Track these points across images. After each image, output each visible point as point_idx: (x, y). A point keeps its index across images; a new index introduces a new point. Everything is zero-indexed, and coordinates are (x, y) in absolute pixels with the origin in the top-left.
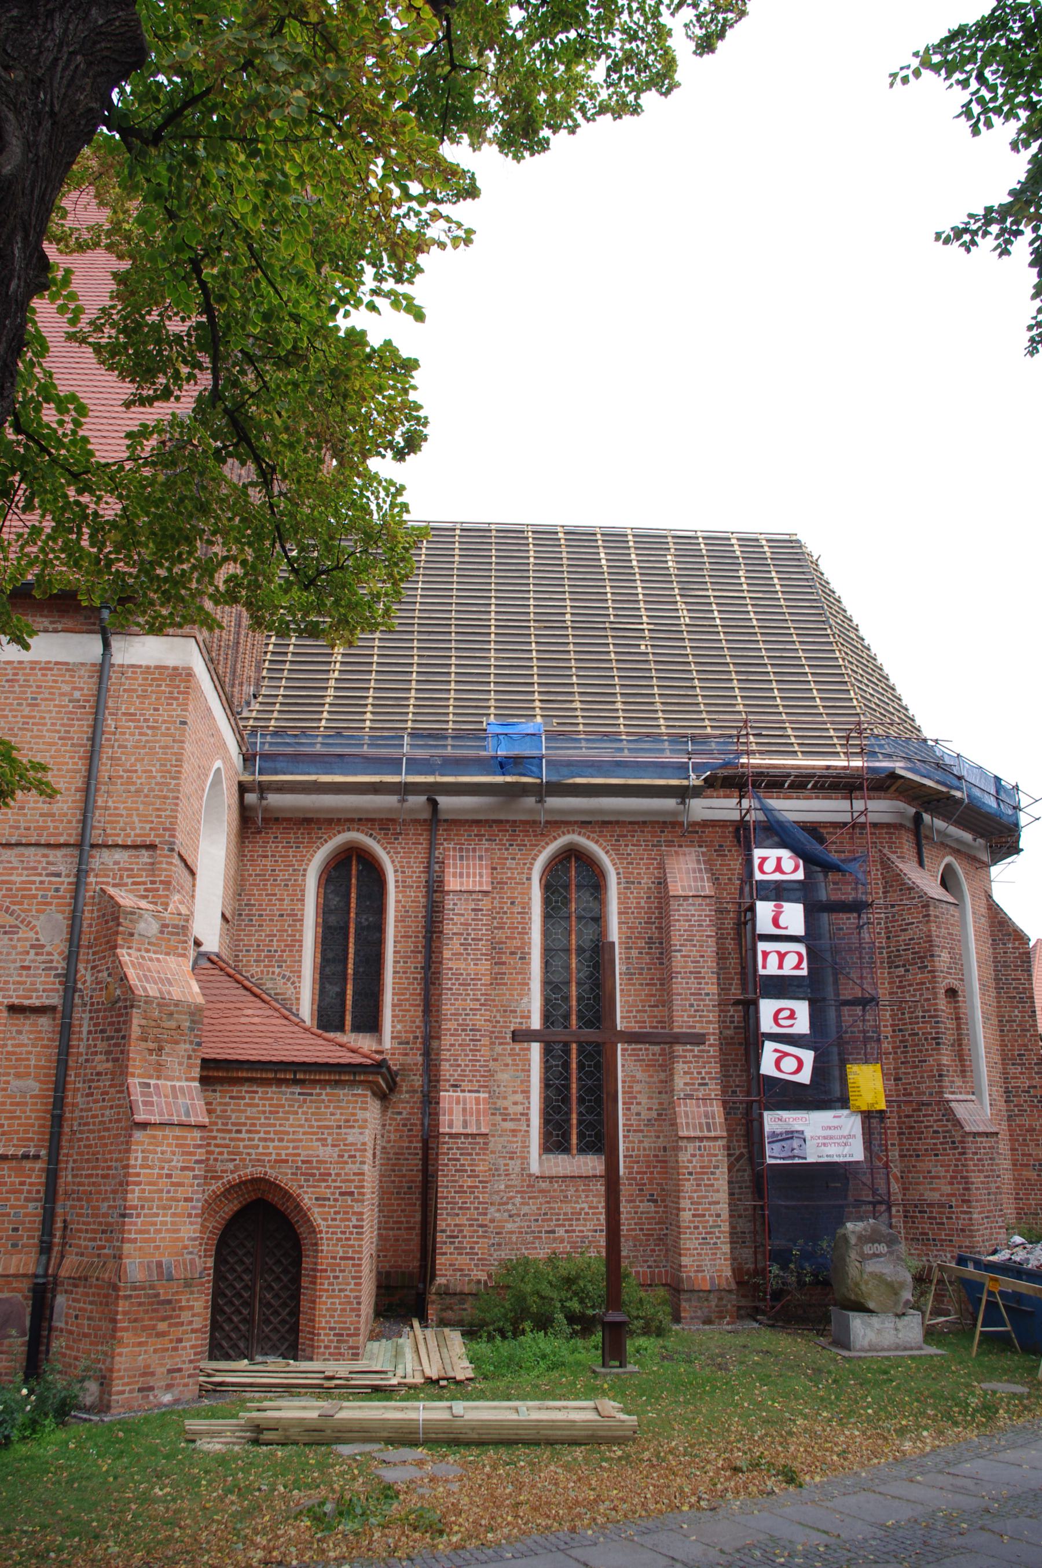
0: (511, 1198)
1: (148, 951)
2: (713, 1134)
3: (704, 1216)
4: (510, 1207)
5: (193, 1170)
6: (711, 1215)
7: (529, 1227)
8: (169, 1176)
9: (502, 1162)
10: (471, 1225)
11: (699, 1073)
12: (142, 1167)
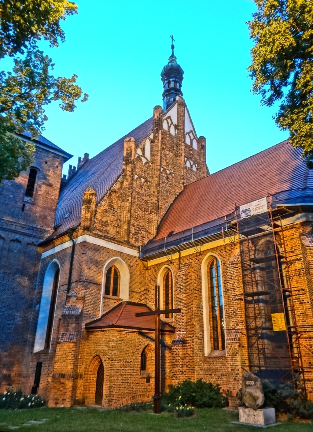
0: (201, 364)
1: (73, 304)
2: (235, 342)
3: (234, 370)
4: (201, 366)
5: (72, 352)
6: (236, 370)
7: (205, 373)
8: (65, 354)
9: (198, 352)
10: (179, 371)
11: (236, 321)
12: (59, 352)
